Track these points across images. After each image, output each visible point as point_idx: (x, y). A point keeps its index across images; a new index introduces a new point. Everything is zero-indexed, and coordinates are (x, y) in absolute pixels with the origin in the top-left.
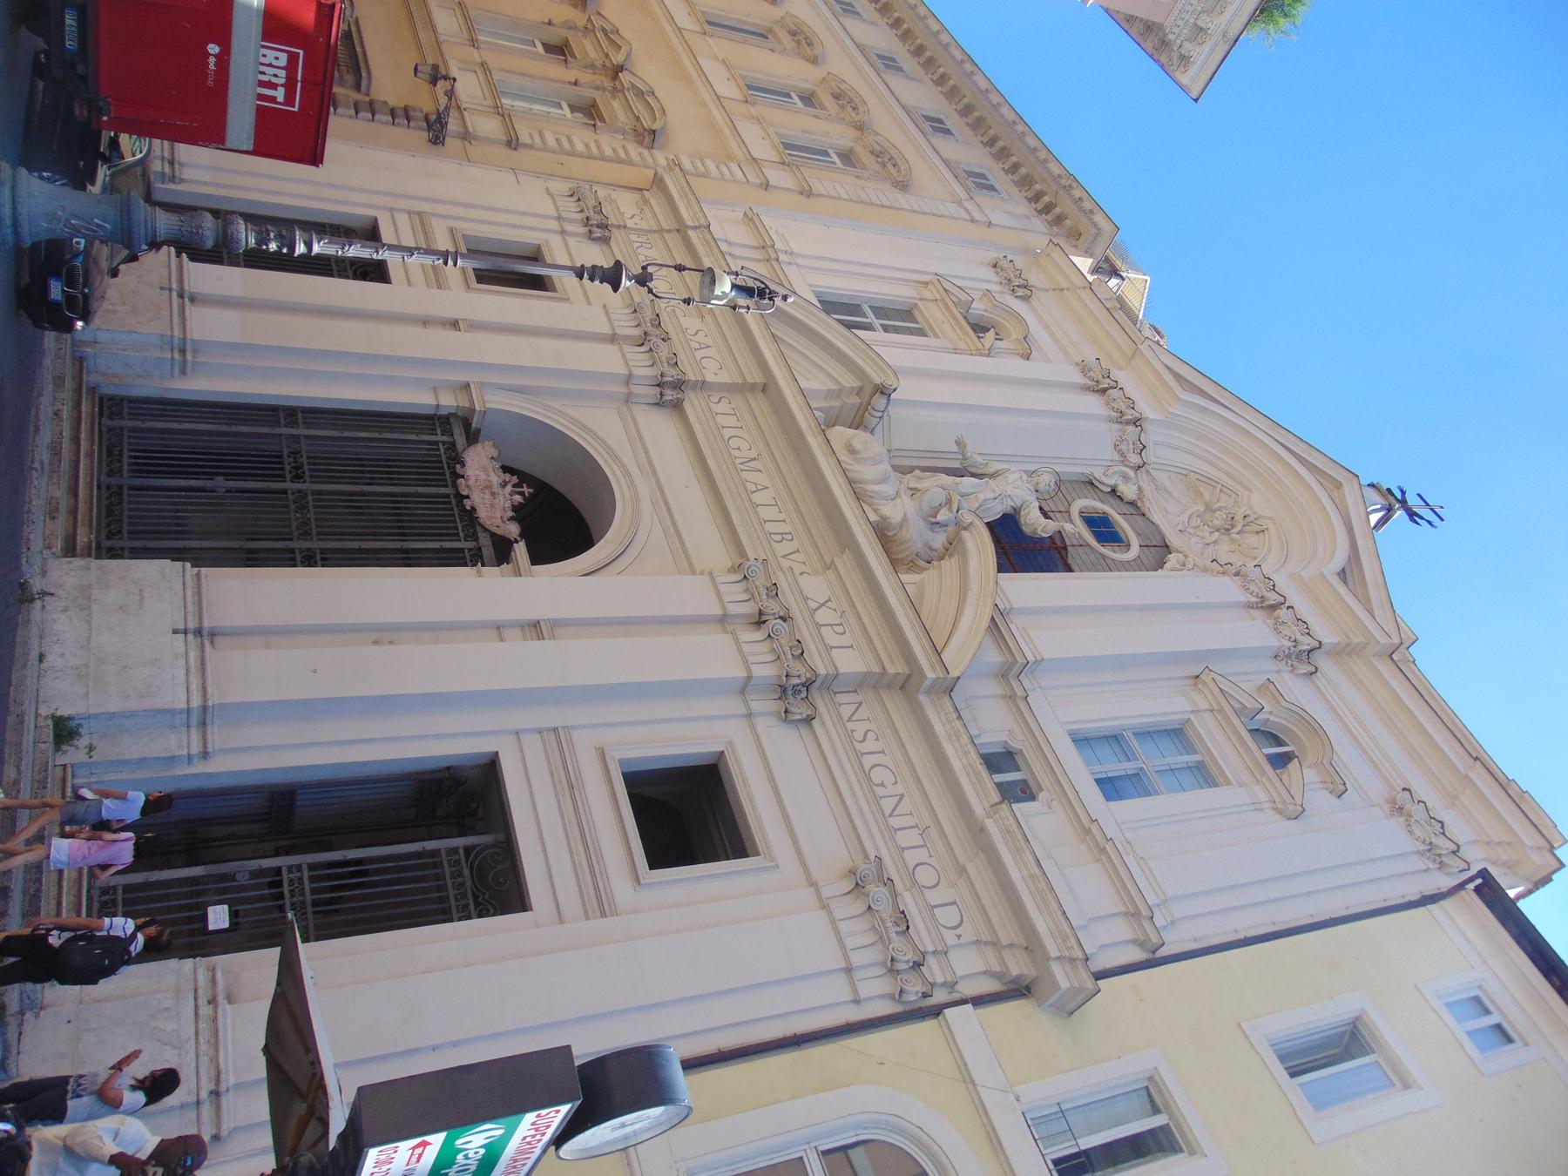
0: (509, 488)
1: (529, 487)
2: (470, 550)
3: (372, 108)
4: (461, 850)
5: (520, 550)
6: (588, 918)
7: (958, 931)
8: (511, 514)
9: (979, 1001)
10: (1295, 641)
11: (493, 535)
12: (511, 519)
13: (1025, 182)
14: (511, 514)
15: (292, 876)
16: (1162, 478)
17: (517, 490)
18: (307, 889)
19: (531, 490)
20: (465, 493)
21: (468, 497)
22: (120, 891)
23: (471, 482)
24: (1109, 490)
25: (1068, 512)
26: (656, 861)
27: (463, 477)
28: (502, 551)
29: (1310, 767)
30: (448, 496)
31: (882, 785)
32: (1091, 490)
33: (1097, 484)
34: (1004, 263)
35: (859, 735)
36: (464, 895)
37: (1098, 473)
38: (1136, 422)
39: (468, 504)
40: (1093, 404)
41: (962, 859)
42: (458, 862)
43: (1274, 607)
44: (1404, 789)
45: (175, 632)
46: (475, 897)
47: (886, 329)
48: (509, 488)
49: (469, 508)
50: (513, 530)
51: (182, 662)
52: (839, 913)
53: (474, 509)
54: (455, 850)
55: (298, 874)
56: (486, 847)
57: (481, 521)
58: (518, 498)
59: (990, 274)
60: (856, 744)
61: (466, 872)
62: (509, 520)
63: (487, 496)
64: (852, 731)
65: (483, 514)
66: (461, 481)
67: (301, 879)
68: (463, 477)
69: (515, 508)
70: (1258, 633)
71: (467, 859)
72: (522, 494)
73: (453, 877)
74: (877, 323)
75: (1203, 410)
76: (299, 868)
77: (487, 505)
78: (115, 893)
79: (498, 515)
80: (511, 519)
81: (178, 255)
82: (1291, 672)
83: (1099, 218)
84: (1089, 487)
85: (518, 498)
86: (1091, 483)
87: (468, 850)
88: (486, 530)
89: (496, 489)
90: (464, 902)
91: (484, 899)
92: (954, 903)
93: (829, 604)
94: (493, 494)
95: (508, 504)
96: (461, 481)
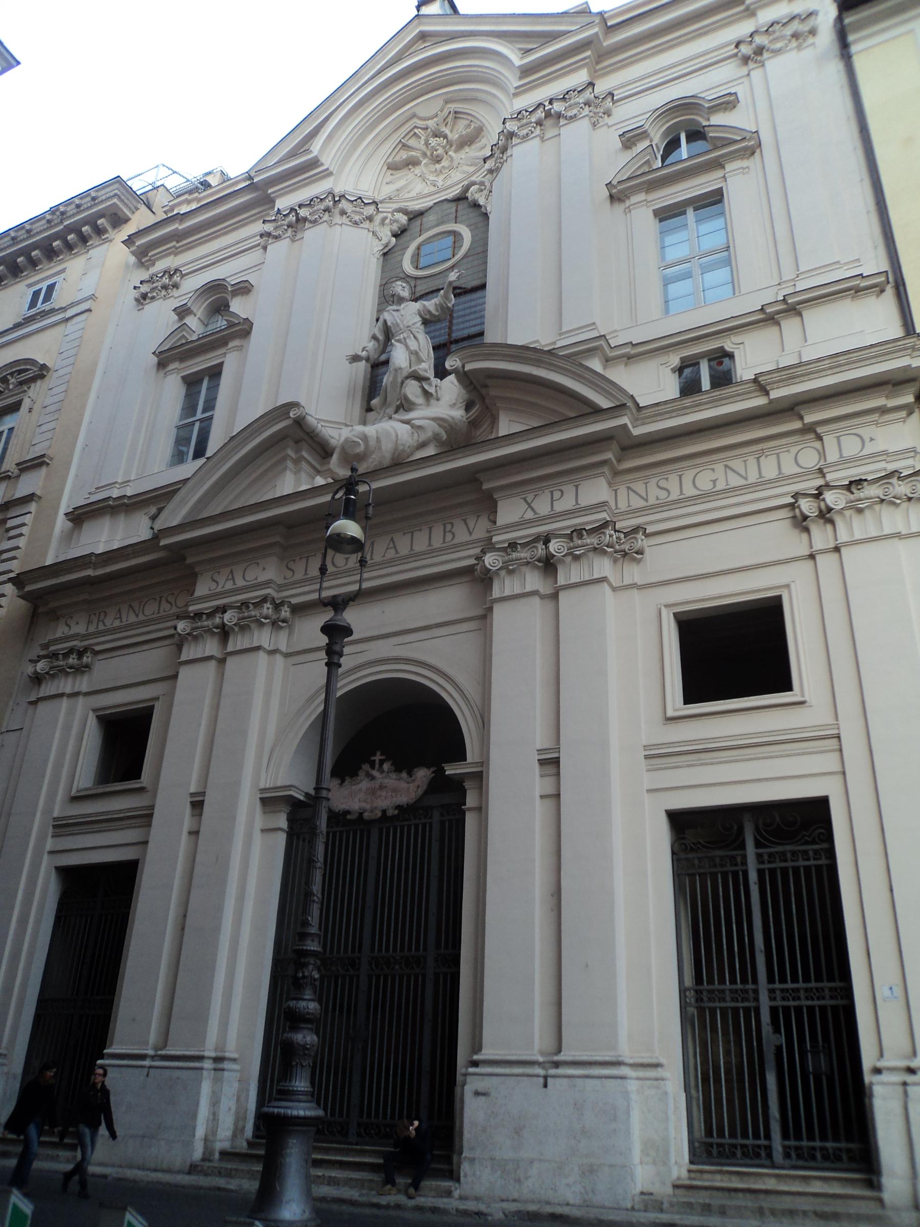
0: (375, 773)
1: (375, 755)
2: (442, 815)
4: (760, 851)
5: (451, 770)
7: (867, 440)
8: (404, 775)
10: (585, 105)
11: (426, 793)
12: (410, 774)
13: (51, 254)
14: (404, 775)
15: (778, 998)
17: (377, 766)
18: (795, 986)
19: (378, 753)
20: (380, 815)
21: (384, 812)
22: (787, 1143)
23: (368, 807)
25: (416, 278)
26: (785, 684)
27: (361, 814)
29: (708, 120)
30: (381, 830)
31: (714, 481)
32: (394, 255)
35: (663, 494)
36: (805, 852)
39: (390, 813)
41: (797, 425)
42: (770, 855)
43: (548, 114)
44: (737, 46)
45: (545, 1086)
46: (807, 843)
48: (375, 773)
49: (396, 812)
50: (423, 775)
51: (579, 1081)
53: (398, 807)
54: (759, 857)
55: (802, 992)
56: (757, 829)
57: (411, 802)
58: (386, 766)
60: (670, 499)
61: (780, 848)
62: (411, 776)
63: (384, 794)
64: (658, 499)
66: (366, 816)
67: (782, 990)
68: (361, 814)
69: (398, 769)
71: (767, 847)
72: (382, 762)
73: (785, 861)
76: (772, 991)
77: (394, 794)
78: (789, 1147)
79: (403, 785)
80: (410, 774)
81: (102, 1057)
83: (102, 195)
84: (390, 257)
86: (385, 254)
87: (758, 844)
88: (420, 799)
89: (376, 784)
90: (811, 853)
91: (804, 835)
92: (838, 438)
93: (529, 500)
94: (382, 787)
95: (394, 776)
96: (366, 816)
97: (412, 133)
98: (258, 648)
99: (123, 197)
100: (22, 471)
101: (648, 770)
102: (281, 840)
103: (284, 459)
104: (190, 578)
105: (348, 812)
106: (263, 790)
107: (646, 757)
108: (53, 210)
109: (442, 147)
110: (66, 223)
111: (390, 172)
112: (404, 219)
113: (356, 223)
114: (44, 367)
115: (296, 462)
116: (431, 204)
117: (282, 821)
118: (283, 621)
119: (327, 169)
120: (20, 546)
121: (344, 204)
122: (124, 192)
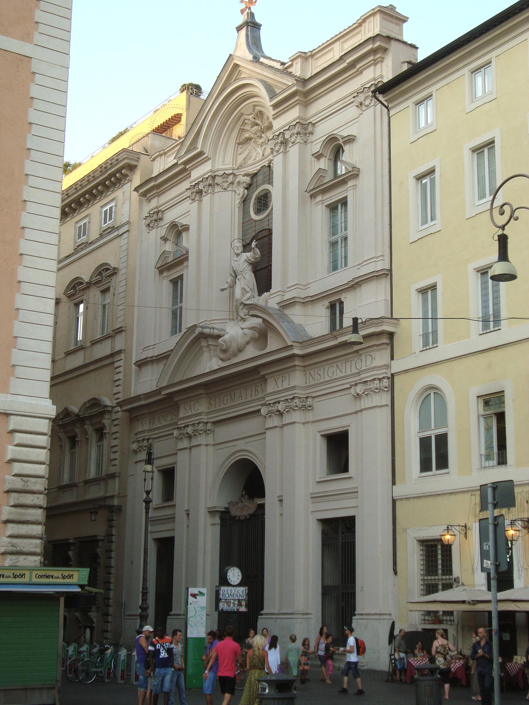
3: (109, 535)
5: (260, 501)
6: (358, 497)
8: (251, 501)
9: (392, 358)
12: (253, 500)
16: (240, 159)
21: (246, 516)
24: (246, 191)
27: (239, 517)
28: (262, 507)
33: (244, 198)
34: (148, 222)
37: (238, 200)
38: (214, 177)
39: (248, 517)
40: (206, 199)
47: (181, 302)
49: (249, 517)
52: (363, 407)
53: (250, 515)
59: (153, 232)
65: (251, 511)
69: (249, 499)
70: (294, 151)
74: (179, 305)
75: (206, 136)
80: (253, 500)
82: (312, 134)
83: (120, 157)
85: (246, 497)
86: (244, 201)
87: (343, 533)
94: (245, 506)
95: (248, 501)
97: (244, 123)
98: (200, 445)
99: (129, 157)
100: (116, 333)
101: (312, 503)
102: (218, 528)
103: (202, 347)
104: (176, 407)
105: (236, 517)
106: (209, 508)
107: (312, 498)
108: (100, 166)
109: (259, 131)
110: (109, 173)
111: (240, 146)
112: (248, 179)
113: (225, 189)
114: (114, 269)
115: (208, 346)
116: (259, 168)
117: (218, 520)
118: (209, 430)
119: (207, 156)
120: (121, 378)
121: (218, 180)
122: (129, 154)
